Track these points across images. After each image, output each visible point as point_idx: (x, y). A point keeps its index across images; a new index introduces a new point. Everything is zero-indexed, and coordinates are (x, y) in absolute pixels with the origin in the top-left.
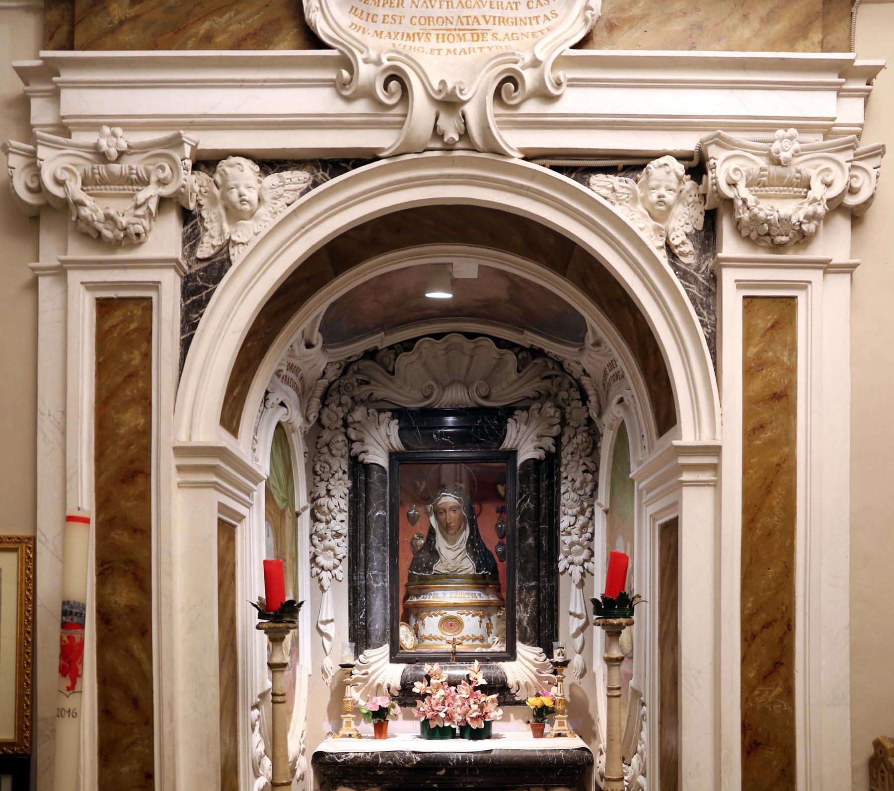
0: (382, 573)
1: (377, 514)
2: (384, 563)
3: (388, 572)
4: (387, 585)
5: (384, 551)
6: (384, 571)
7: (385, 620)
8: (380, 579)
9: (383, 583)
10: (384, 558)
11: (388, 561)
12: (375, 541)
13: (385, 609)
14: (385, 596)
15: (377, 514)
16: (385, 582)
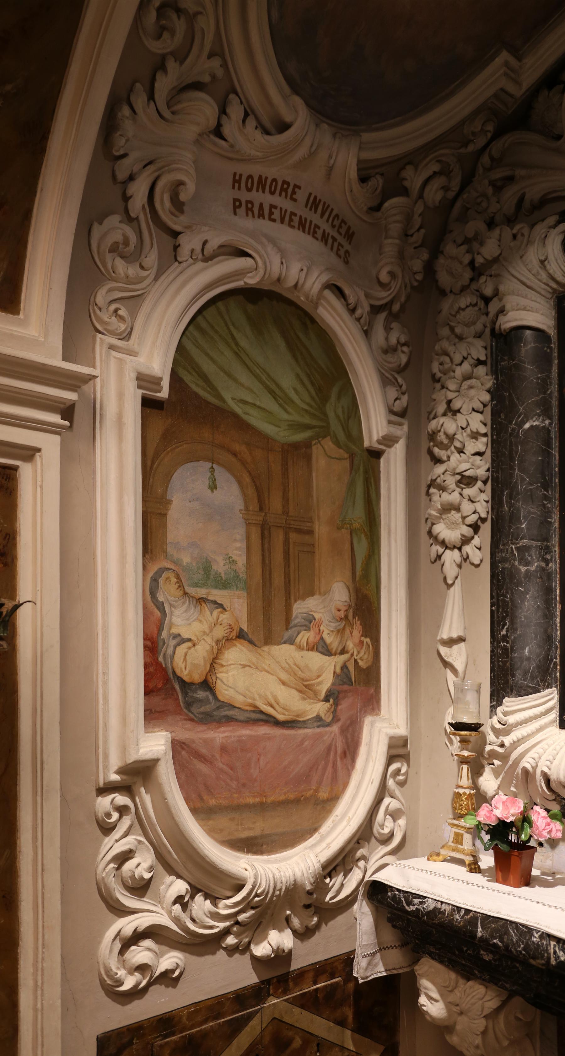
0: (539, 543)
1: (527, 426)
2: (545, 523)
3: (555, 540)
4: (554, 566)
5: (546, 497)
6: (546, 539)
7: (549, 639)
8: (534, 555)
9: (543, 564)
10: (547, 513)
11: (555, 519)
12: (523, 480)
13: (548, 615)
14: (549, 591)
15: (527, 426)
16: (547, 562)
